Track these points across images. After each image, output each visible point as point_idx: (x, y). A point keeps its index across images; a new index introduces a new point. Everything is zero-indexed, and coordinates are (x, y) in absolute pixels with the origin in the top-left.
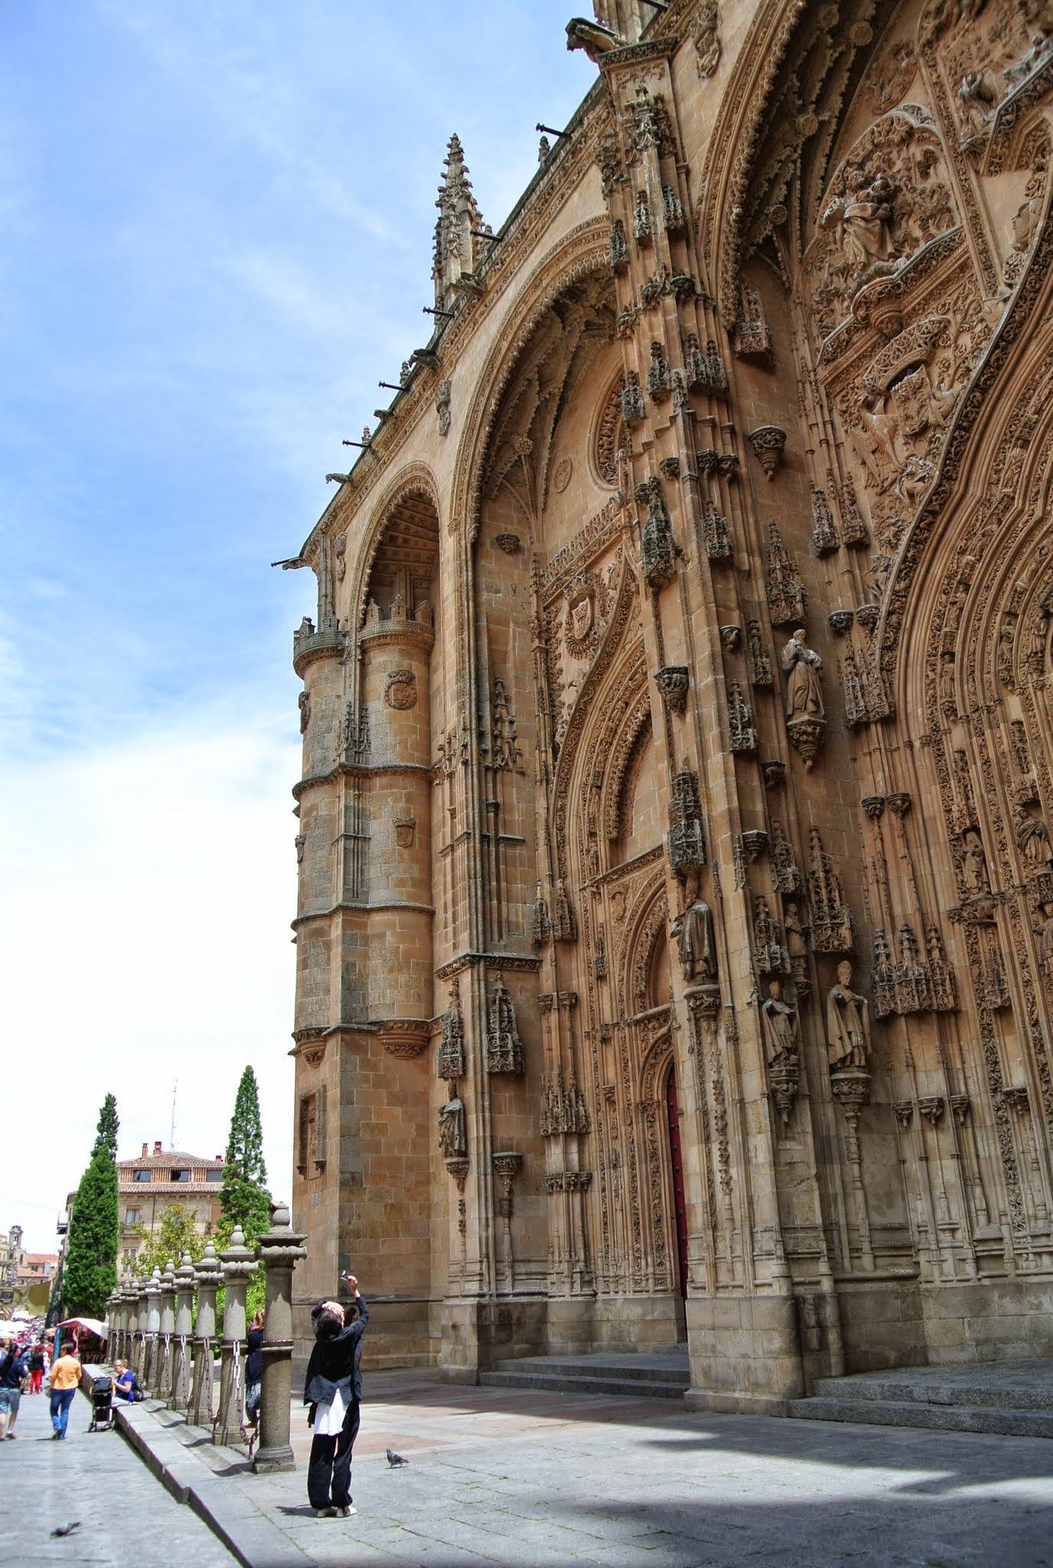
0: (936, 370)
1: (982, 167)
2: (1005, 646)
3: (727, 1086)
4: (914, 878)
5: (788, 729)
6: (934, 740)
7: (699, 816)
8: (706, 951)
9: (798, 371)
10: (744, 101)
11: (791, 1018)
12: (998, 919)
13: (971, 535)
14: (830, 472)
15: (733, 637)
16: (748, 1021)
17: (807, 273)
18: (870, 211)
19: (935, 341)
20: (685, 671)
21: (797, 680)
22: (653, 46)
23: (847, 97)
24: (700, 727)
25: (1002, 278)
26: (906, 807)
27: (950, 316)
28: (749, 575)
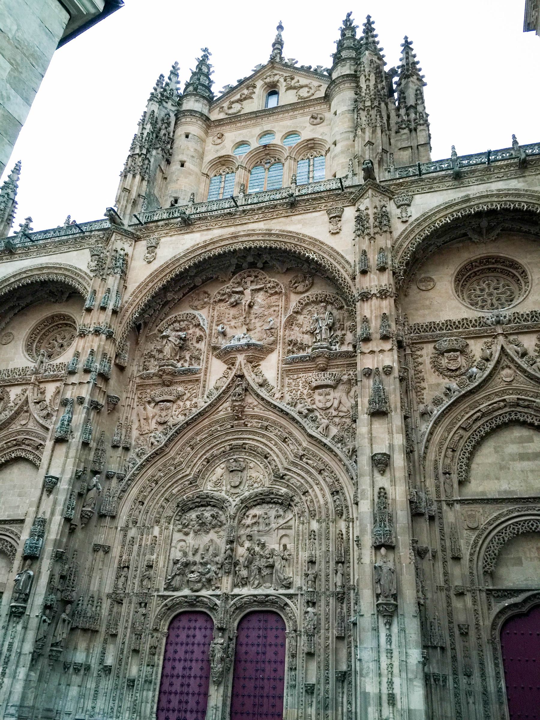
0: (175, 406)
1: (215, 353)
2: (162, 510)
3: (16, 645)
4: (101, 578)
5: (82, 511)
6: (125, 529)
7: (42, 536)
8: (28, 591)
9: (130, 374)
10: (156, 281)
11: (49, 624)
12: (123, 602)
13: (165, 465)
14: (127, 418)
15: (80, 474)
16: (34, 623)
17: (146, 341)
18: (177, 343)
19: (179, 397)
20: (57, 479)
21: (92, 494)
22: (133, 234)
23: (184, 295)
24: (55, 503)
25: (206, 393)
26: (107, 550)
27: (186, 392)
28: (90, 449)
